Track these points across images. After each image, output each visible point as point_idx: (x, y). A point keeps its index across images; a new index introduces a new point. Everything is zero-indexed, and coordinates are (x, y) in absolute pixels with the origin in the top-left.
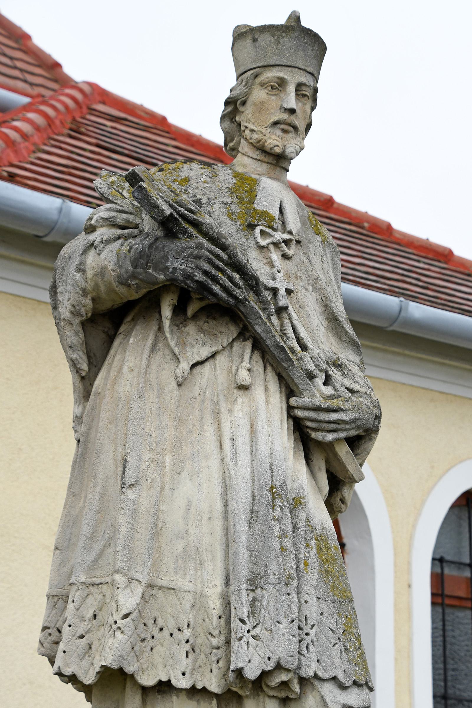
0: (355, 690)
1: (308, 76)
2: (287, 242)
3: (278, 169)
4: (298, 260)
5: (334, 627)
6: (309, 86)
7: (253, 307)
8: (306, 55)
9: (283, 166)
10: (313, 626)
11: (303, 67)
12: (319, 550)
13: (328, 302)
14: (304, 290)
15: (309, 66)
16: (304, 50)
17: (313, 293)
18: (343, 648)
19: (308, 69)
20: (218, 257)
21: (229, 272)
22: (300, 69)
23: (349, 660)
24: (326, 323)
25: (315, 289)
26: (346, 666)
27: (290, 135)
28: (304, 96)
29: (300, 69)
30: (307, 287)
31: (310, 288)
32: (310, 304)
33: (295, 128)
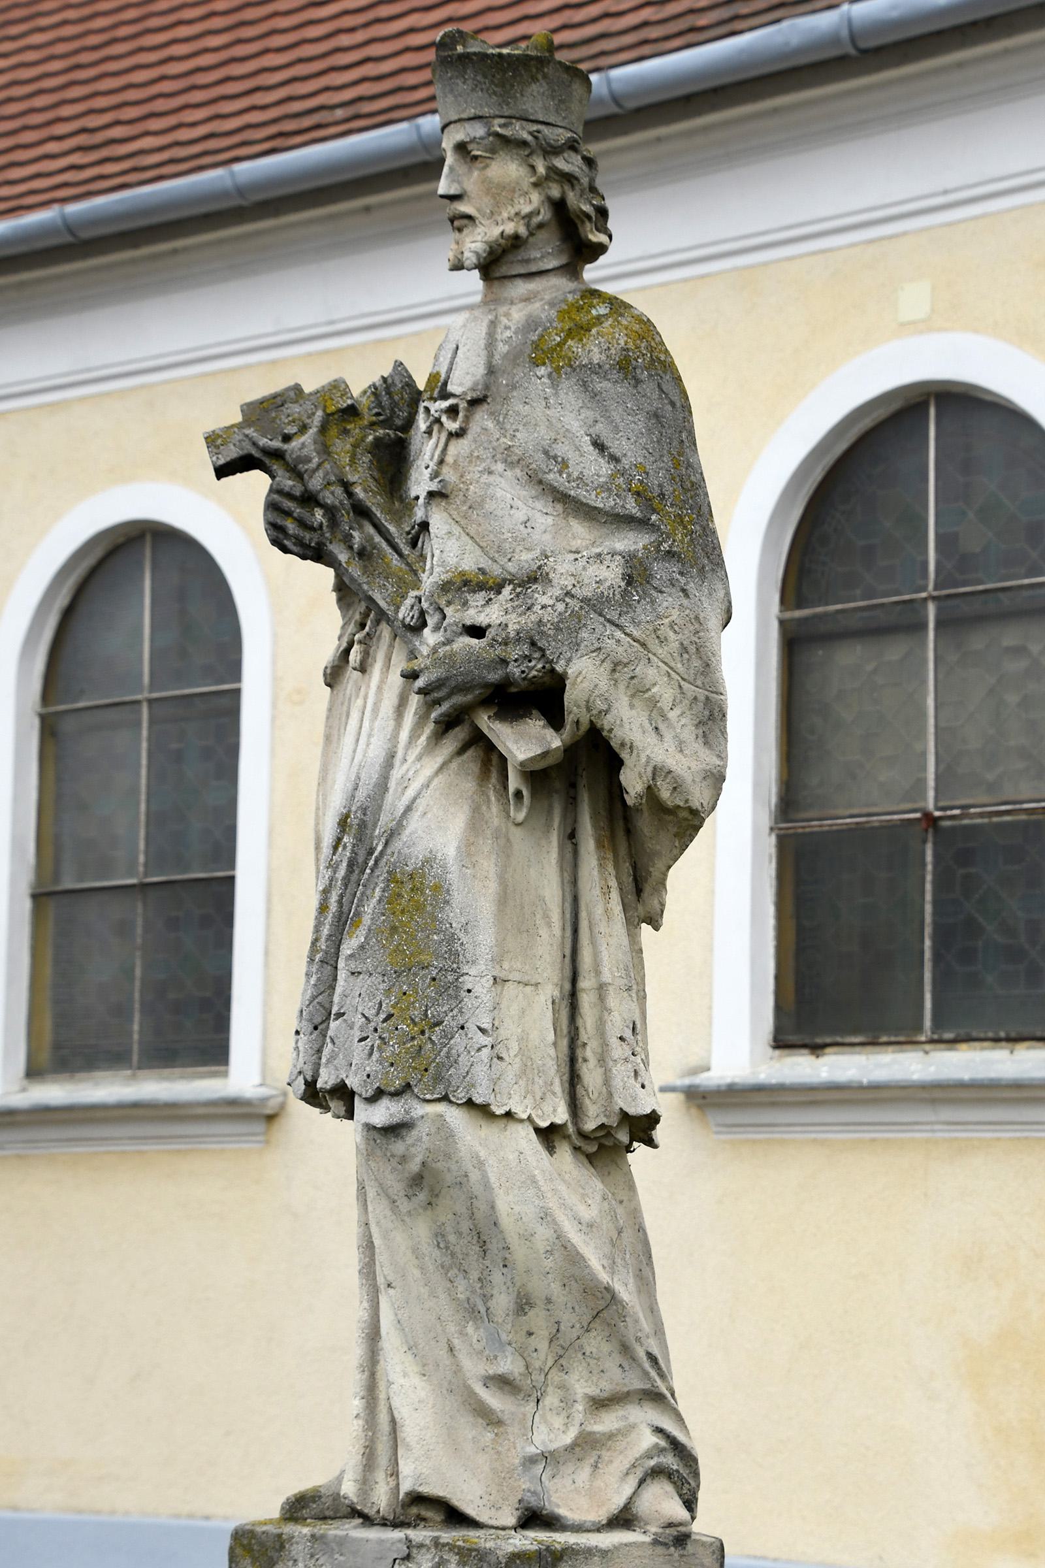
0: (385, 1102)
1: (467, 125)
2: (453, 411)
3: (496, 283)
4: (479, 430)
5: (370, 1013)
6: (473, 140)
7: (331, 552)
8: (455, 97)
9: (498, 275)
10: (340, 1015)
11: (456, 117)
12: (391, 899)
13: (540, 475)
14: (485, 476)
15: (464, 111)
16: (452, 91)
17: (509, 473)
18: (378, 1042)
19: (464, 116)
20: (289, 496)
21: (297, 511)
22: (455, 122)
23: (380, 1061)
24: (559, 507)
25: (510, 464)
26: (372, 1066)
27: (466, 231)
28: (476, 158)
29: (455, 122)
30: (493, 468)
31: (500, 467)
32: (499, 493)
33: (469, 217)
